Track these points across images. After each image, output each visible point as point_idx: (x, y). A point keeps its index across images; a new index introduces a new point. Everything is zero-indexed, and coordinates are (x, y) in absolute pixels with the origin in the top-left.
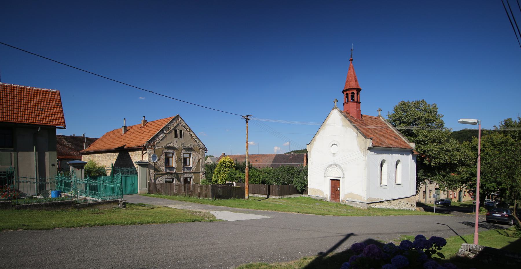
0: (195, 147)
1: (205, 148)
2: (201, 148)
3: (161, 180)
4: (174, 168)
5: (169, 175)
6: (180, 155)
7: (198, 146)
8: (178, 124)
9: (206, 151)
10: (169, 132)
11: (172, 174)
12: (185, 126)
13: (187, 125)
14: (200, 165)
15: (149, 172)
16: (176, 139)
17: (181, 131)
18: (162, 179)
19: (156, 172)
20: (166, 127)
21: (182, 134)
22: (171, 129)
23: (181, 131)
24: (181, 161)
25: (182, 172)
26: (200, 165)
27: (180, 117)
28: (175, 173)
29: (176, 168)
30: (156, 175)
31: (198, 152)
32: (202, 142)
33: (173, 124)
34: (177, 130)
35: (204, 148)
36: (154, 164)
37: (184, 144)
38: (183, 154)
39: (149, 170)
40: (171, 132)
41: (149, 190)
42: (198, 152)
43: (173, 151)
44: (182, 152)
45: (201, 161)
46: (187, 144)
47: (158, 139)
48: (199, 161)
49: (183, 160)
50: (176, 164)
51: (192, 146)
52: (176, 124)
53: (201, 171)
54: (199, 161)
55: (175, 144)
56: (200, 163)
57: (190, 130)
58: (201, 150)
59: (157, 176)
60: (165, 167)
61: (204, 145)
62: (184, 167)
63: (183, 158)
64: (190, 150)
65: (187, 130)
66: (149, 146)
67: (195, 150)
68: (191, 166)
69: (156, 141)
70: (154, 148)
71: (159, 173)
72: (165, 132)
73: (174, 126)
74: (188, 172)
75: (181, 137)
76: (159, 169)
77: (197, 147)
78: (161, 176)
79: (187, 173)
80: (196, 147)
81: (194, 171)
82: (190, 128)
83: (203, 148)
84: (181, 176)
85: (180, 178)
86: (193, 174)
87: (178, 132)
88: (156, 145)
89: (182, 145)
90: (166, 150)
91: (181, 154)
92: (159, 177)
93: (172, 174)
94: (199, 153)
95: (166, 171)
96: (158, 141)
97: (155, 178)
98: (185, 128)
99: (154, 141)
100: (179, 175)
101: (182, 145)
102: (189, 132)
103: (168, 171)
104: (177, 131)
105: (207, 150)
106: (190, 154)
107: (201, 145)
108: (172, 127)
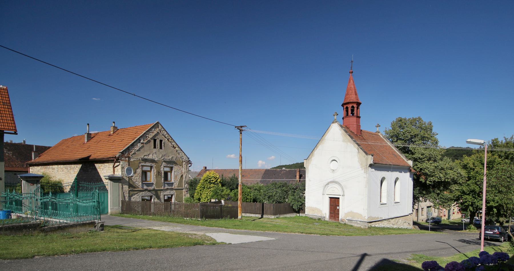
0: (177, 160)
1: (190, 161)
2: (185, 161)
3: (137, 198)
4: (153, 184)
5: (146, 192)
6: (160, 169)
7: (181, 159)
8: (158, 133)
9: (190, 165)
10: (147, 142)
11: (150, 191)
12: (166, 135)
13: (169, 134)
14: (184, 181)
15: (123, 188)
16: (155, 150)
17: (161, 141)
18: (138, 197)
19: (131, 189)
20: (144, 136)
21: (163, 144)
22: (150, 138)
23: (161, 141)
24: (161, 175)
25: (162, 188)
26: (184, 181)
27: (161, 125)
28: (154, 190)
29: (155, 183)
30: (130, 192)
31: (181, 165)
32: (186, 155)
33: (152, 133)
34: (156, 140)
35: (188, 161)
36: (129, 179)
37: (164, 155)
38: (163, 167)
39: (122, 186)
40: (149, 142)
41: (122, 210)
42: (181, 165)
43: (151, 164)
44: (163, 165)
45: (184, 177)
46: (168, 156)
47: (134, 149)
48: (182, 176)
49: (163, 175)
50: (155, 179)
51: (174, 159)
52: (155, 132)
53: (184, 187)
54: (182, 176)
55: (154, 156)
56: (183, 179)
57: (172, 140)
58: (184, 163)
59: (132, 193)
60: (142, 183)
61: (187, 157)
62: (164, 182)
63: (163, 172)
64: (171, 163)
65: (168, 140)
66: (123, 157)
67: (177, 163)
68: (173, 181)
69: (132, 152)
70: (129, 160)
71: (134, 189)
72: (142, 141)
73: (153, 134)
74: (169, 189)
75: (161, 148)
76: (134, 185)
77: (179, 160)
78: (137, 193)
79: (167, 189)
80: (178, 159)
81: (176, 188)
82: (171, 138)
83: (186, 161)
84: (161, 193)
85: (159, 195)
86: (174, 191)
87: (158, 142)
88: (131, 157)
89: (162, 157)
90: (143, 163)
91: (161, 167)
92: (135, 194)
93: (150, 191)
94: (183, 167)
95: (142, 187)
96: (134, 152)
97: (130, 195)
98: (166, 138)
99: (128, 152)
100: (159, 192)
101: (162, 157)
102: (170, 142)
103: (145, 187)
104: (157, 141)
105: (192, 164)
106: (172, 168)
107: (185, 158)
108: (151, 136)
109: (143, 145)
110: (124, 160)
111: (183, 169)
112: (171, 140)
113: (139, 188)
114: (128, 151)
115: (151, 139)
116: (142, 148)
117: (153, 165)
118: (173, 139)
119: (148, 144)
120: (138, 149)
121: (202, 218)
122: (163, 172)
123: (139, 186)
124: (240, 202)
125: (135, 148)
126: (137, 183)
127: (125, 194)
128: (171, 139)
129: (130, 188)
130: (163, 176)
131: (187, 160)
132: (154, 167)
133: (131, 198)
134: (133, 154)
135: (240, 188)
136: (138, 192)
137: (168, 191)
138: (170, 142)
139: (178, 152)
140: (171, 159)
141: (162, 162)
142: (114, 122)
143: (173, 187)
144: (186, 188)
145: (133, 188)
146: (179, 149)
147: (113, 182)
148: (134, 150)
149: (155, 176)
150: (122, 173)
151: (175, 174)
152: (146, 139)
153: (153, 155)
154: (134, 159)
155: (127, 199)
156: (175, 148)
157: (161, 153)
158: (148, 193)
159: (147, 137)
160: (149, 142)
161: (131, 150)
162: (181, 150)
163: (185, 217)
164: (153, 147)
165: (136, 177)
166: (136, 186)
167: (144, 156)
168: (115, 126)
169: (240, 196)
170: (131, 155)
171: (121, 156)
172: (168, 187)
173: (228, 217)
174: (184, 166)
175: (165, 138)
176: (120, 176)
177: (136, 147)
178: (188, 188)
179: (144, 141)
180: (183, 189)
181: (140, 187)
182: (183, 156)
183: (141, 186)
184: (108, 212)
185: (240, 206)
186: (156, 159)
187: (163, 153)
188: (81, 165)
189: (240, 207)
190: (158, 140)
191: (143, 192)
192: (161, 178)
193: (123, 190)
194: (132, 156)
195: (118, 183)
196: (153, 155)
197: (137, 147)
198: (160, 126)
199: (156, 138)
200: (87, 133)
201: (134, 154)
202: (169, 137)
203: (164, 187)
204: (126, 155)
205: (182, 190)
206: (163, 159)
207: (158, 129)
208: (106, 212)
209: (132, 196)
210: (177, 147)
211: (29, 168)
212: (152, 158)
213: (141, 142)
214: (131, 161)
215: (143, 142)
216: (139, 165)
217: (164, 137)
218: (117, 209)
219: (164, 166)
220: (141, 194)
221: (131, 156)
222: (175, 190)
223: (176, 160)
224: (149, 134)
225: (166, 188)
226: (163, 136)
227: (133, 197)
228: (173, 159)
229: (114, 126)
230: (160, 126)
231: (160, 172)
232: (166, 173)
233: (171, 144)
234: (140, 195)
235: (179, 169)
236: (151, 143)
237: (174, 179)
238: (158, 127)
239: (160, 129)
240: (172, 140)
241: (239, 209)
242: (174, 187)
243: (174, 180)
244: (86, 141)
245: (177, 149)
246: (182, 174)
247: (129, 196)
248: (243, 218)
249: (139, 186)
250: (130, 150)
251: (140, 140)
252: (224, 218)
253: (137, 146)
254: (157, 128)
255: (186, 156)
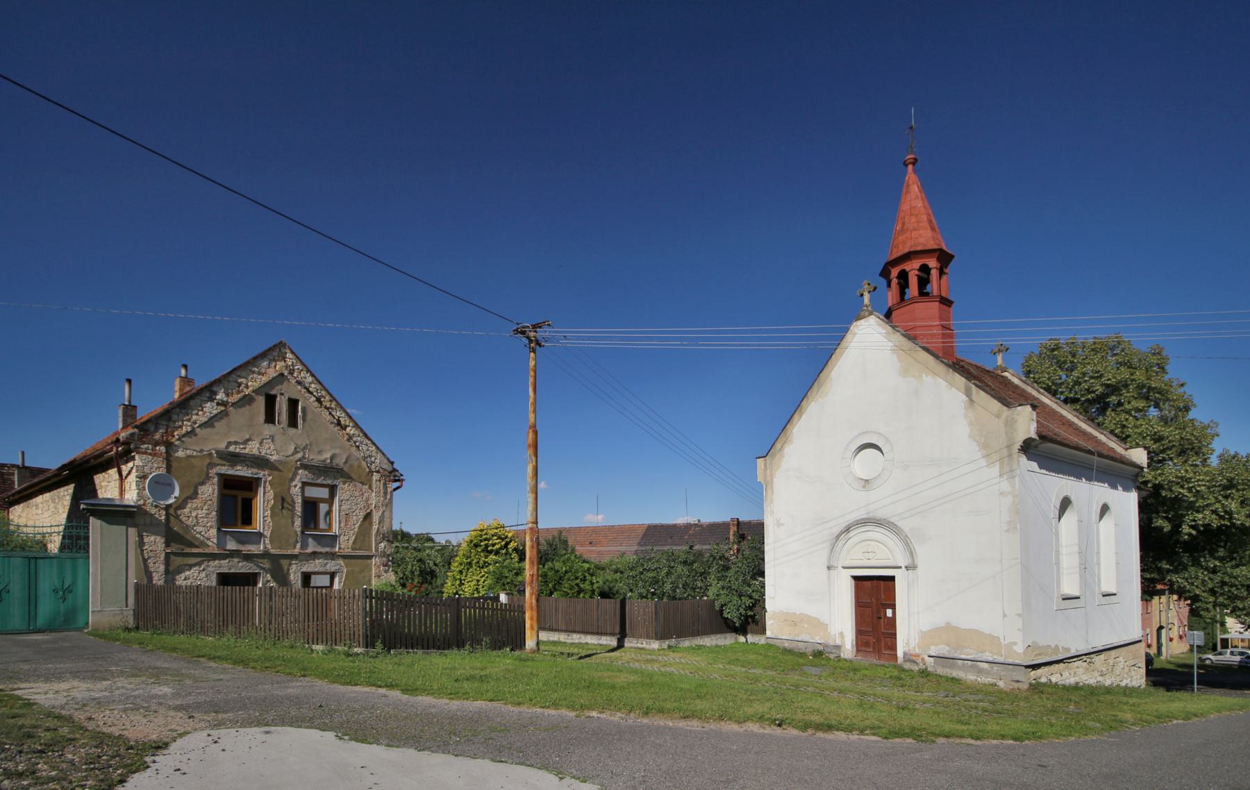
0: (351, 466)
1: (395, 470)
2: (378, 472)
3: (199, 576)
4: (260, 535)
5: (236, 560)
6: (289, 489)
7: (364, 464)
8: (282, 375)
9: (397, 484)
10: (240, 400)
11: (248, 557)
12: (313, 386)
13: (320, 383)
14: (374, 532)
15: (141, 543)
16: (269, 430)
17: (293, 403)
18: (203, 574)
19: (175, 548)
20: (227, 379)
21: (300, 413)
22: (251, 389)
23: (293, 403)
24: (293, 510)
25: (297, 551)
26: (374, 532)
27: (293, 353)
28: (266, 555)
29: (267, 533)
30: (172, 557)
31: (366, 482)
32: (381, 451)
33: (259, 373)
34: (274, 397)
35: (391, 472)
36: (167, 515)
37: (305, 448)
38: (300, 485)
39: (141, 537)
40: (247, 400)
41: (137, 615)
42: (366, 482)
43: (255, 470)
44: (298, 477)
45: (376, 517)
46: (320, 452)
47: (189, 420)
48: (368, 516)
49: (299, 508)
50: (269, 519)
51: (340, 461)
52: (272, 373)
53: (377, 550)
54: (368, 516)
55: (267, 446)
56: (371, 524)
57: (334, 403)
58: (376, 476)
59: (177, 561)
60: (219, 530)
61: (388, 459)
62: (303, 532)
63: (299, 500)
64: (331, 473)
65: (318, 400)
66: (144, 443)
67: (353, 475)
68: (335, 529)
69: (181, 427)
70: (167, 452)
71: (188, 550)
72: (221, 396)
73: (265, 379)
74: (321, 553)
75: (293, 423)
76: (189, 537)
77: (360, 466)
78: (199, 564)
79: (315, 555)
80: (356, 463)
81: (348, 551)
82: (331, 396)
83: (385, 470)
84: (290, 564)
85: (286, 571)
86: (341, 562)
87: (282, 406)
88: (177, 443)
89: (296, 452)
90: (224, 465)
91: (294, 483)
92: (191, 566)
93: (248, 557)
94: (370, 487)
95: (220, 545)
96: (189, 429)
97: (171, 569)
98: (311, 393)
99: (168, 426)
100: (284, 563)
101: (296, 452)
102: (327, 408)
103: (232, 545)
104: (278, 399)
105: (403, 480)
106: (333, 489)
107: (378, 461)
108: (253, 382)
109: (223, 408)
110: (149, 451)
111: (374, 494)
112: (331, 401)
113: (208, 546)
114: (164, 423)
115: (256, 391)
116: (222, 418)
117: (261, 476)
118: (335, 400)
119: (243, 409)
120: (204, 419)
121: (369, 643)
122: (300, 501)
123: (208, 539)
124: (532, 588)
125: (194, 417)
126: (199, 529)
127: (151, 565)
128: (328, 398)
129: (172, 544)
130: (300, 514)
131: (388, 467)
132: (265, 482)
133: (174, 579)
134: (184, 436)
135: (532, 540)
136: (203, 561)
137: (317, 561)
138: (327, 408)
139: (355, 442)
140: (329, 461)
141: (297, 469)
142: (185, 366)
143: (337, 550)
144: (384, 554)
145: (182, 546)
146: (357, 433)
147: (104, 523)
148: (189, 424)
149: (269, 512)
150: (138, 493)
151: (343, 507)
152: (239, 392)
153: (261, 443)
154: (188, 452)
155: (158, 579)
156: (345, 428)
157: (292, 440)
158: (240, 564)
159: (240, 384)
160: (247, 400)
161: (178, 421)
162: (366, 436)
163: (315, 642)
164: (262, 417)
165: (196, 509)
166: (197, 538)
167: (230, 444)
168: (186, 375)
169: (531, 568)
170: (177, 437)
171: (136, 437)
172: (319, 547)
173: (484, 643)
174: (374, 486)
175: (307, 395)
176: (132, 504)
177: (197, 414)
178: (389, 555)
179: (227, 395)
180: (372, 556)
181: (210, 544)
182: (374, 454)
183: (215, 541)
184: (87, 623)
185: (531, 604)
186: (274, 458)
187: (299, 442)
188: (72, 486)
189: (532, 608)
190: (283, 397)
191: (222, 562)
192: (293, 518)
193: (142, 551)
194: (183, 442)
195: (125, 527)
196: (261, 443)
197: (200, 413)
198: (289, 355)
199: (273, 392)
200: (124, 405)
201: (188, 434)
202: (324, 393)
203: (302, 548)
204: (157, 436)
205: (369, 561)
206: (299, 460)
207: (280, 365)
208: (81, 623)
209: (179, 571)
210: (351, 424)
211: (6, 512)
212: (257, 453)
213: (218, 397)
214: (178, 457)
215: (225, 399)
216: (208, 473)
217: (303, 390)
218: (114, 615)
219: (305, 480)
220: (215, 567)
221: (179, 439)
222: (344, 557)
223: (348, 465)
224: (248, 375)
225: (309, 550)
226: (299, 387)
227: (183, 576)
228: (335, 462)
229: (186, 377)
230: (289, 355)
231: (289, 500)
232: (311, 507)
233: (330, 413)
234: (210, 569)
235: (357, 494)
236: (255, 405)
237: (340, 523)
238: (284, 359)
239: (290, 363)
240: (334, 403)
241: (527, 615)
242: (340, 548)
243: (339, 527)
244: (121, 426)
245: (352, 432)
246: (368, 511)
247: (167, 572)
248: (542, 647)
249: (208, 539)
250: (175, 422)
251: (215, 393)
252: (467, 647)
253: (202, 410)
254: (278, 360)
255: (384, 454)
